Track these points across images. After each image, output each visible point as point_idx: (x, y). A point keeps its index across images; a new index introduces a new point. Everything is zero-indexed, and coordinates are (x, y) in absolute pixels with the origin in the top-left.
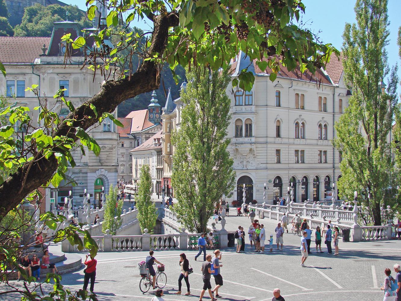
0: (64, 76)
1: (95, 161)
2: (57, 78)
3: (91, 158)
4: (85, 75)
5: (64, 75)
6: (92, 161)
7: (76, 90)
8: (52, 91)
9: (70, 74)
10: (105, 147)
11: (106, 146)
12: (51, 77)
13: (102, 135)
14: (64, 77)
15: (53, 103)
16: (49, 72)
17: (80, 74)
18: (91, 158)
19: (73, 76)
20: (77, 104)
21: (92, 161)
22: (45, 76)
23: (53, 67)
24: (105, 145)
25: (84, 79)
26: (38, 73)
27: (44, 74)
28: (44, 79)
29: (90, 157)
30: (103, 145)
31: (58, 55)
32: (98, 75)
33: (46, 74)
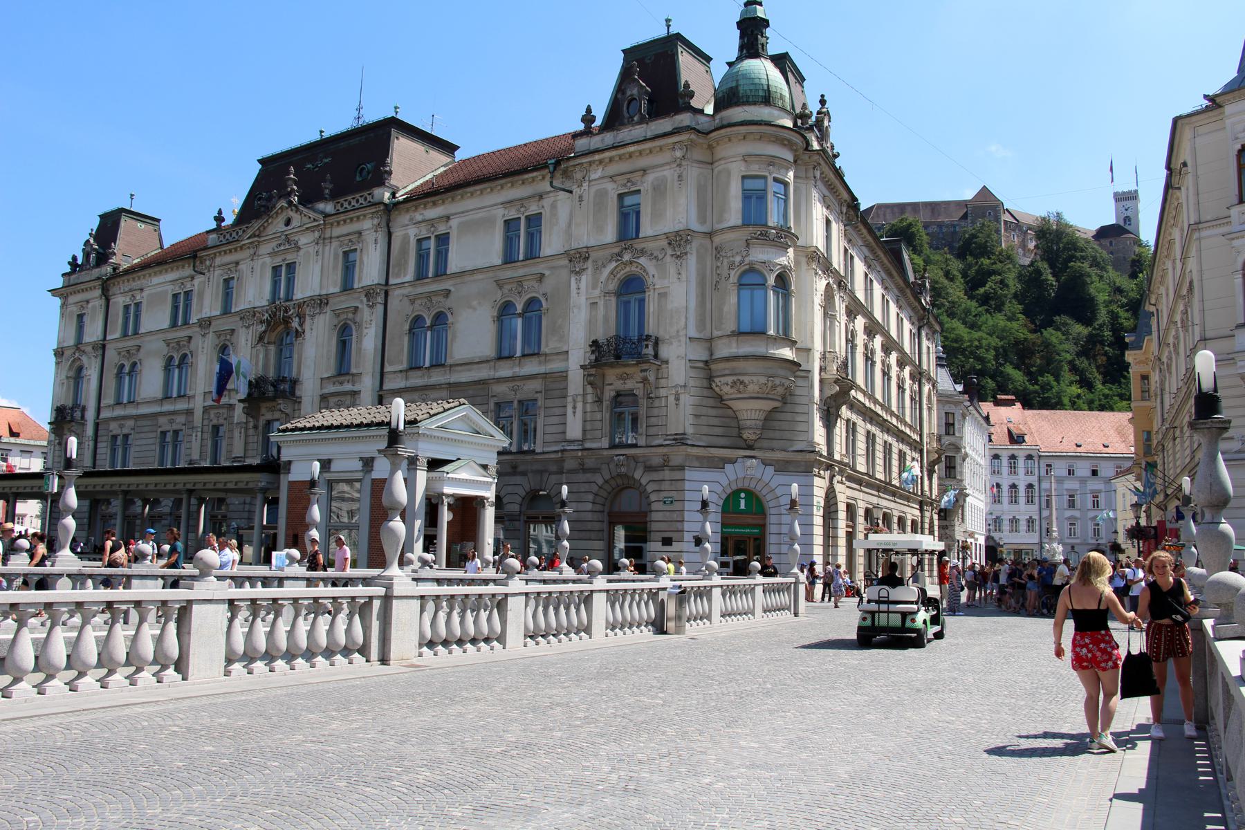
0: (629, 180)
1: (719, 431)
2: (612, 190)
3: (704, 420)
4: (680, 165)
5: (629, 176)
6: (705, 430)
7: (657, 215)
8: (600, 229)
9: (644, 171)
10: (742, 383)
11: (746, 379)
12: (597, 190)
13: (734, 345)
14: (629, 184)
15: (600, 264)
16: (593, 176)
17: (668, 167)
18: (704, 420)
19: (651, 177)
20: (660, 257)
21: (705, 430)
22: (583, 189)
23: (601, 162)
24: (741, 378)
25: (679, 177)
26: (567, 185)
27: (580, 186)
28: (581, 199)
29: (696, 416)
30: (735, 378)
31: (617, 124)
32: (723, 162)
33: (585, 185)
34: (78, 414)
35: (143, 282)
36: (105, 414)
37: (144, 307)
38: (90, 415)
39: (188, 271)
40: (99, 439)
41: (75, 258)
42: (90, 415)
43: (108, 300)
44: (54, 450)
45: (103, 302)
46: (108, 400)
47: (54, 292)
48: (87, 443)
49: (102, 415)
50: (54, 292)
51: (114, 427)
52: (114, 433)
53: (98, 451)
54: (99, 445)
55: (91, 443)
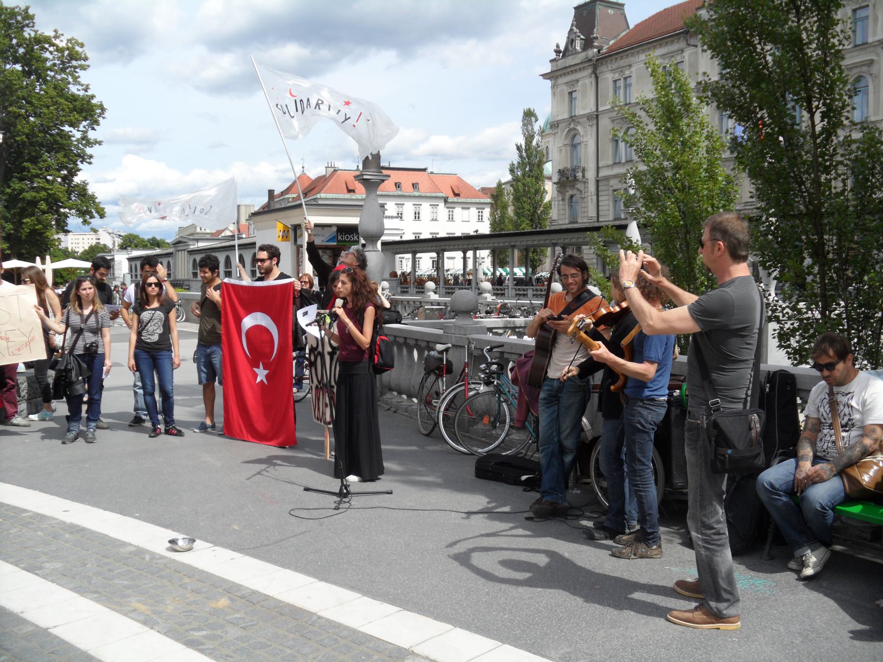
34: (579, 175)
35: (631, 60)
36: (603, 173)
37: (633, 80)
38: (591, 175)
39: (682, 44)
40: (600, 194)
41: (558, 46)
42: (591, 175)
43: (597, 78)
44: (559, 205)
45: (593, 80)
46: (605, 161)
47: (545, 76)
48: (590, 198)
49: (601, 174)
50: (545, 76)
51: (615, 183)
52: (615, 187)
53: (600, 204)
54: (601, 198)
55: (595, 198)
